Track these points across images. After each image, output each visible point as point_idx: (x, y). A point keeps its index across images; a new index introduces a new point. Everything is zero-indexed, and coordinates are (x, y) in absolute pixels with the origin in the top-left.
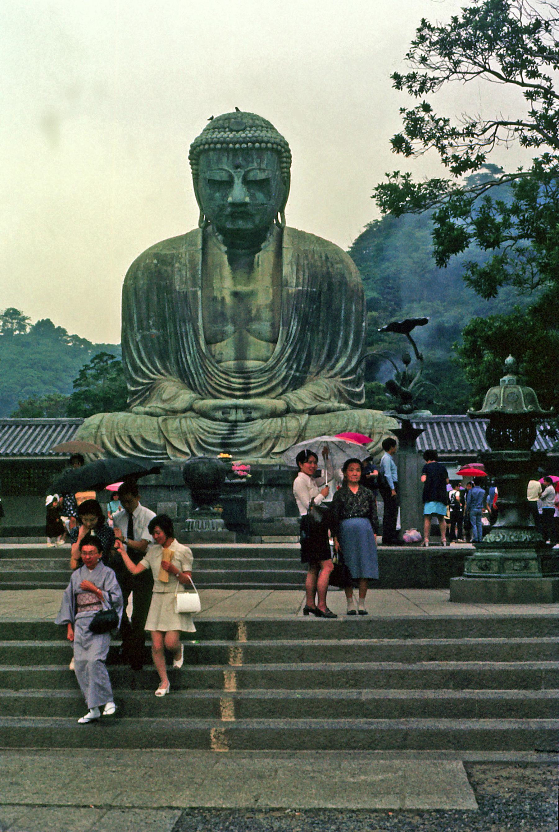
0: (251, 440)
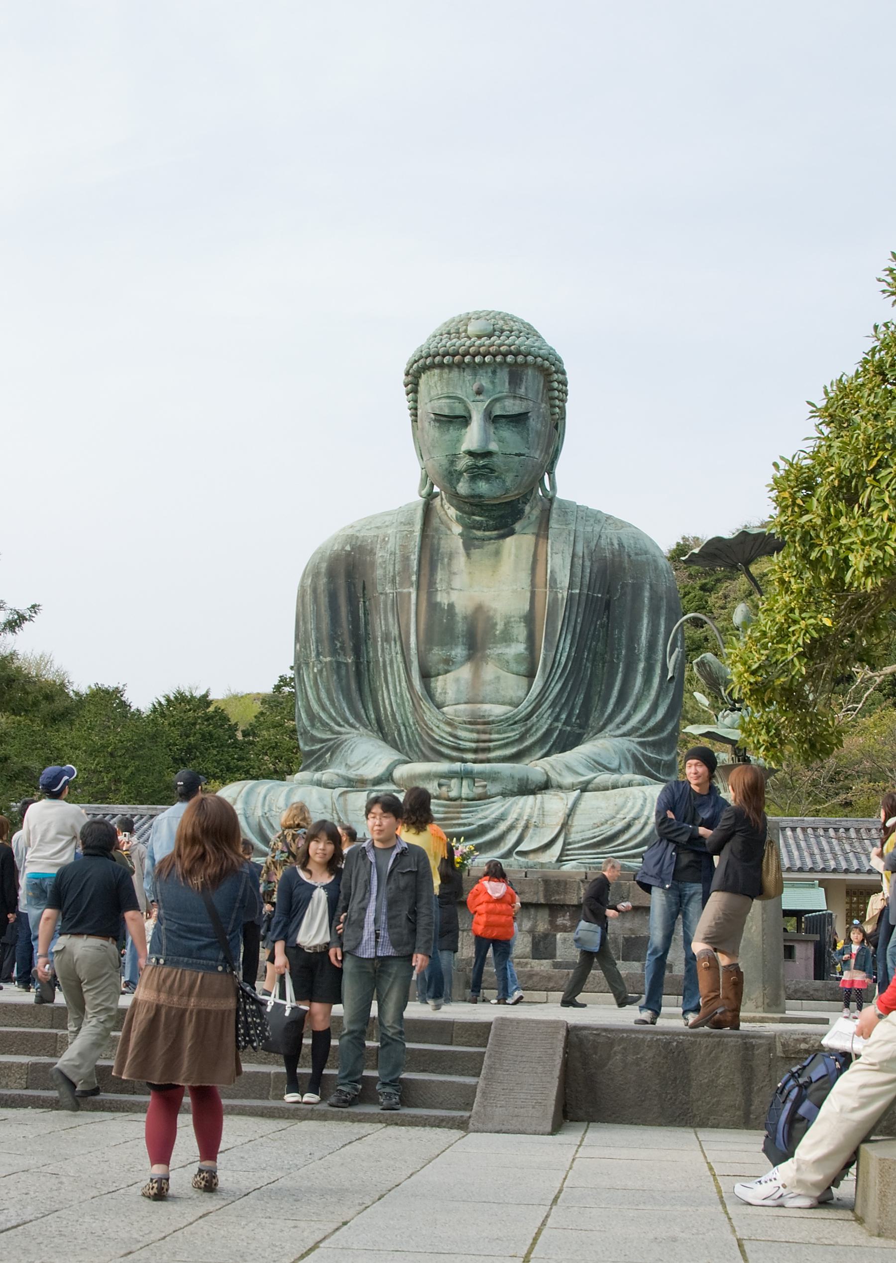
0: (484, 829)
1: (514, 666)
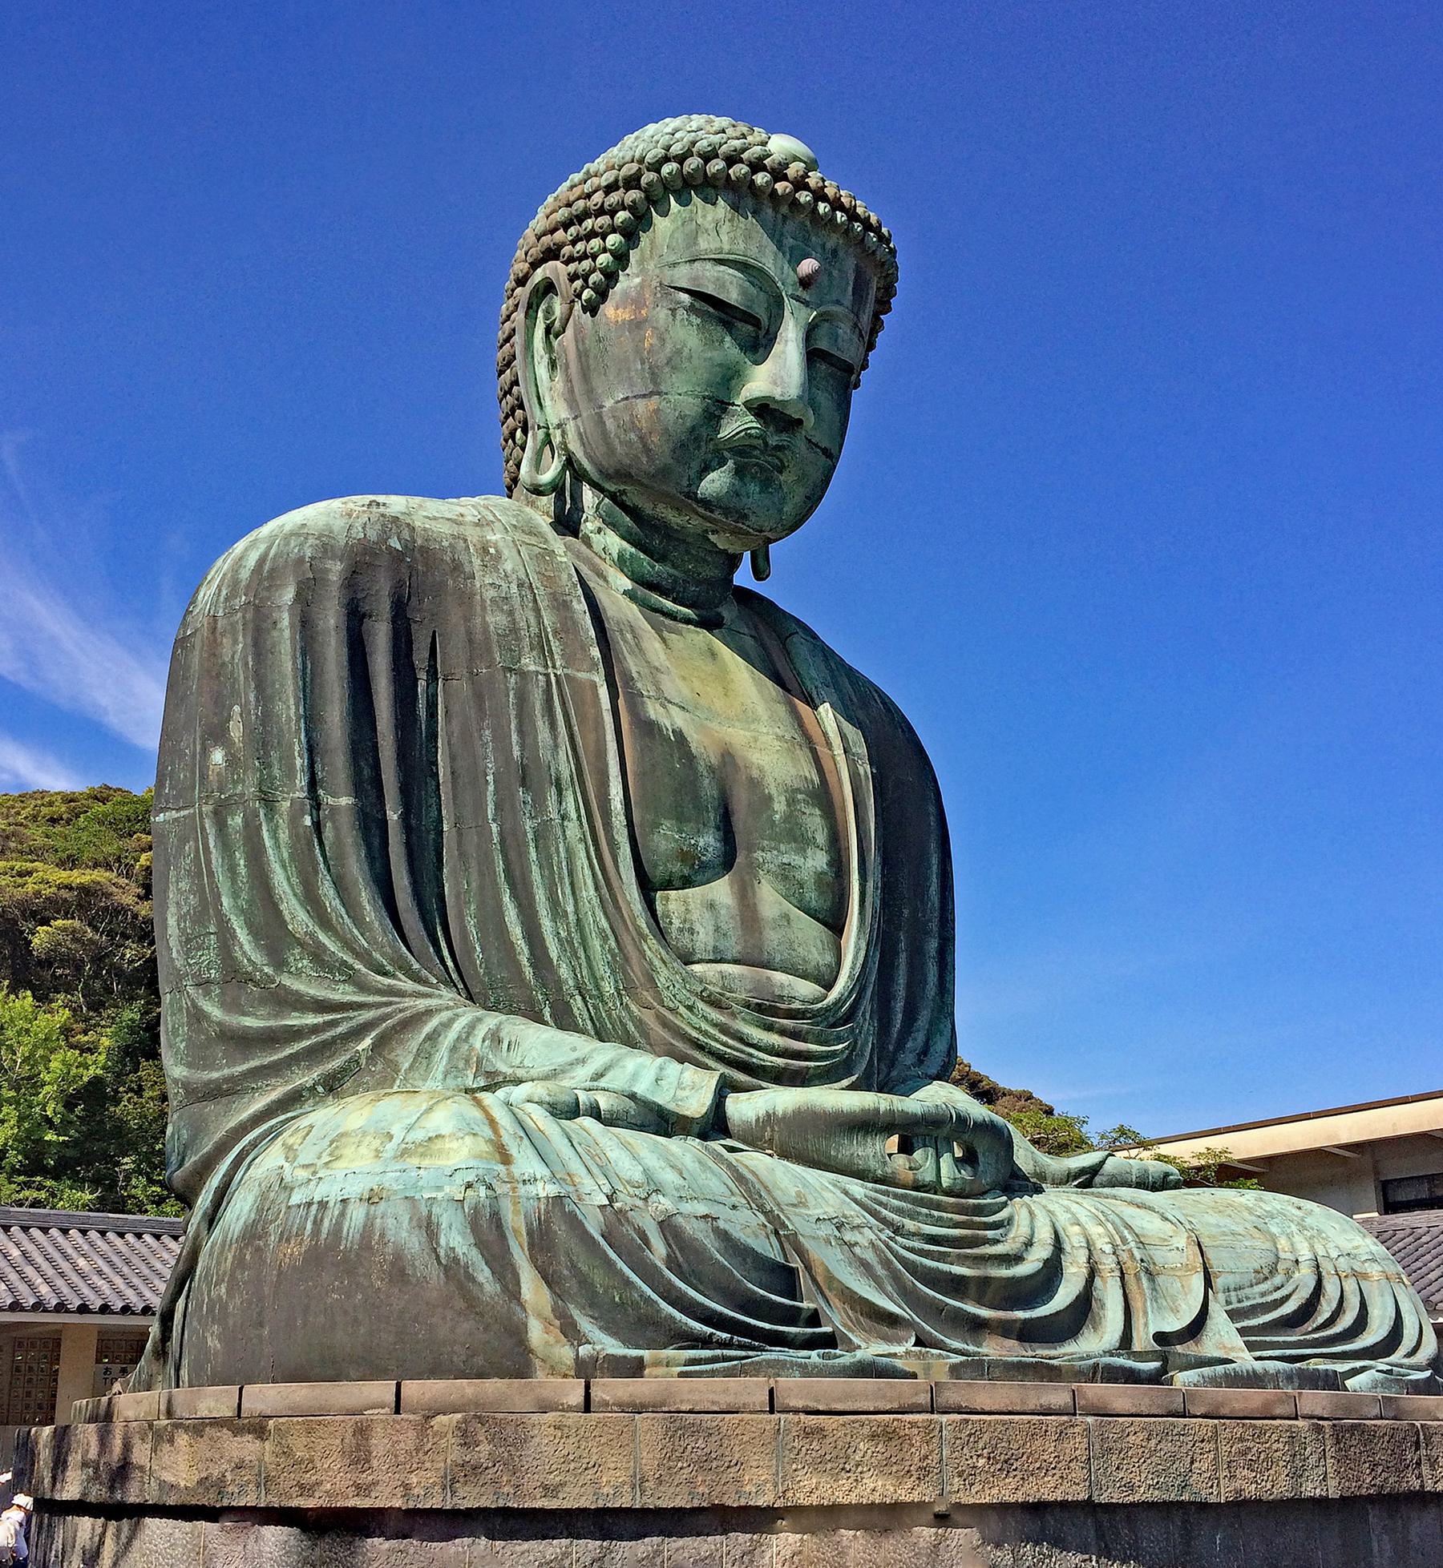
1: (812, 896)
